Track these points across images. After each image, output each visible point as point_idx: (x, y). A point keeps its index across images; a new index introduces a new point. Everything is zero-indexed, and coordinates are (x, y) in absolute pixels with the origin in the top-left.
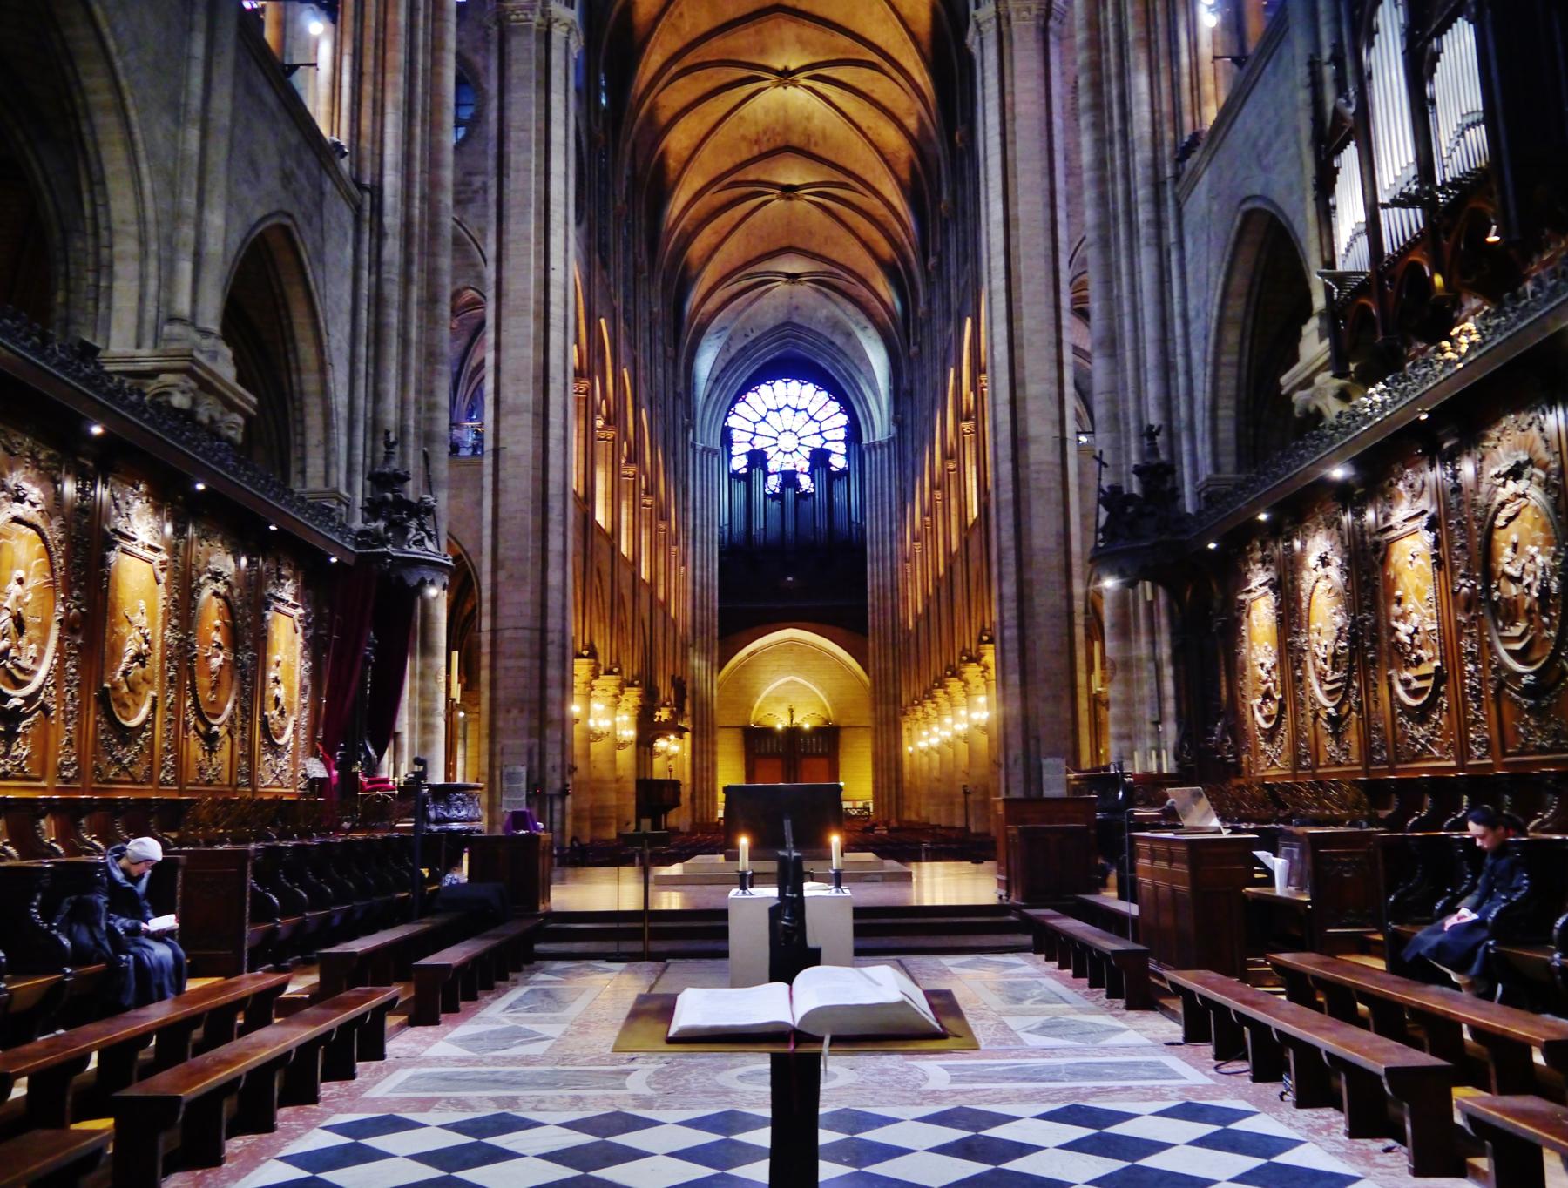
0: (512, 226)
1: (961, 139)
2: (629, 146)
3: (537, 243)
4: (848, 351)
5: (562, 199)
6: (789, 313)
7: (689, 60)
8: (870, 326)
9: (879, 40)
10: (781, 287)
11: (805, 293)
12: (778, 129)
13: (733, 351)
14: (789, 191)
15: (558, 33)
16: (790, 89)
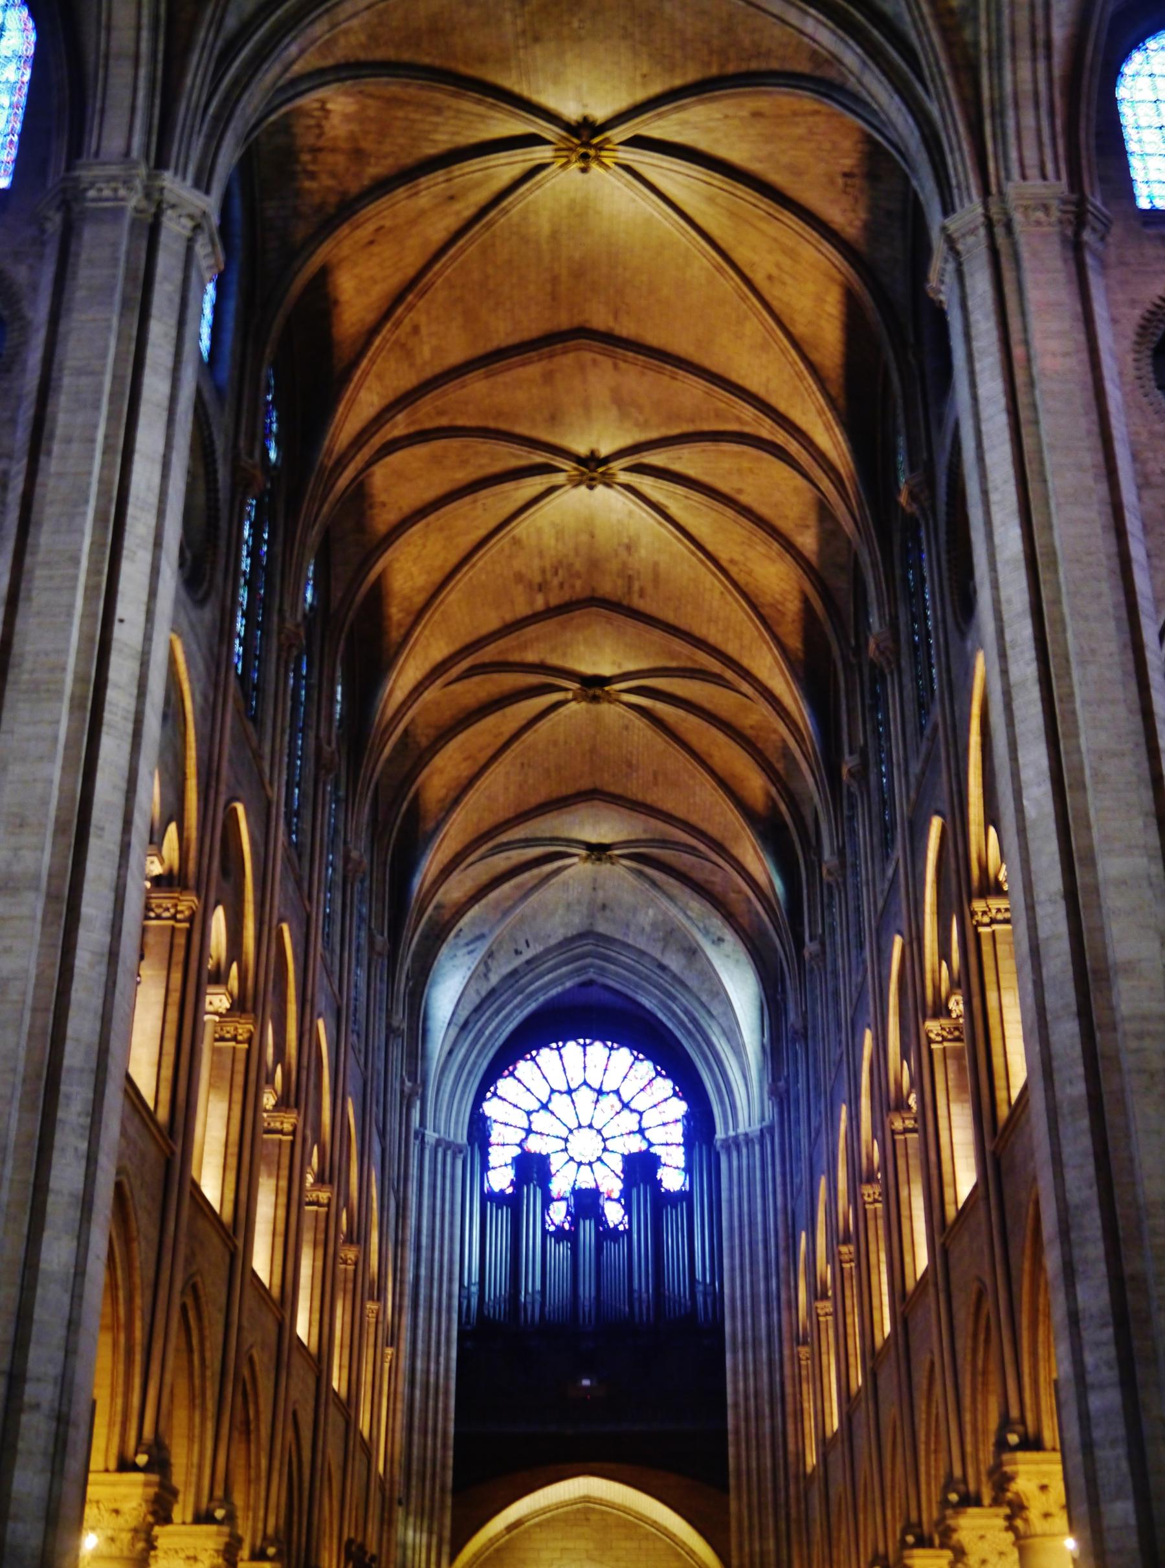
0: (45, 538)
1: (913, 496)
2: (314, 536)
3: (93, 571)
4: (693, 983)
5: (153, 499)
6: (592, 916)
7: (426, 414)
8: (729, 936)
9: (754, 384)
10: (579, 869)
11: (618, 876)
12: (578, 565)
13: (494, 979)
14: (594, 687)
15: (174, 228)
16: (600, 489)
